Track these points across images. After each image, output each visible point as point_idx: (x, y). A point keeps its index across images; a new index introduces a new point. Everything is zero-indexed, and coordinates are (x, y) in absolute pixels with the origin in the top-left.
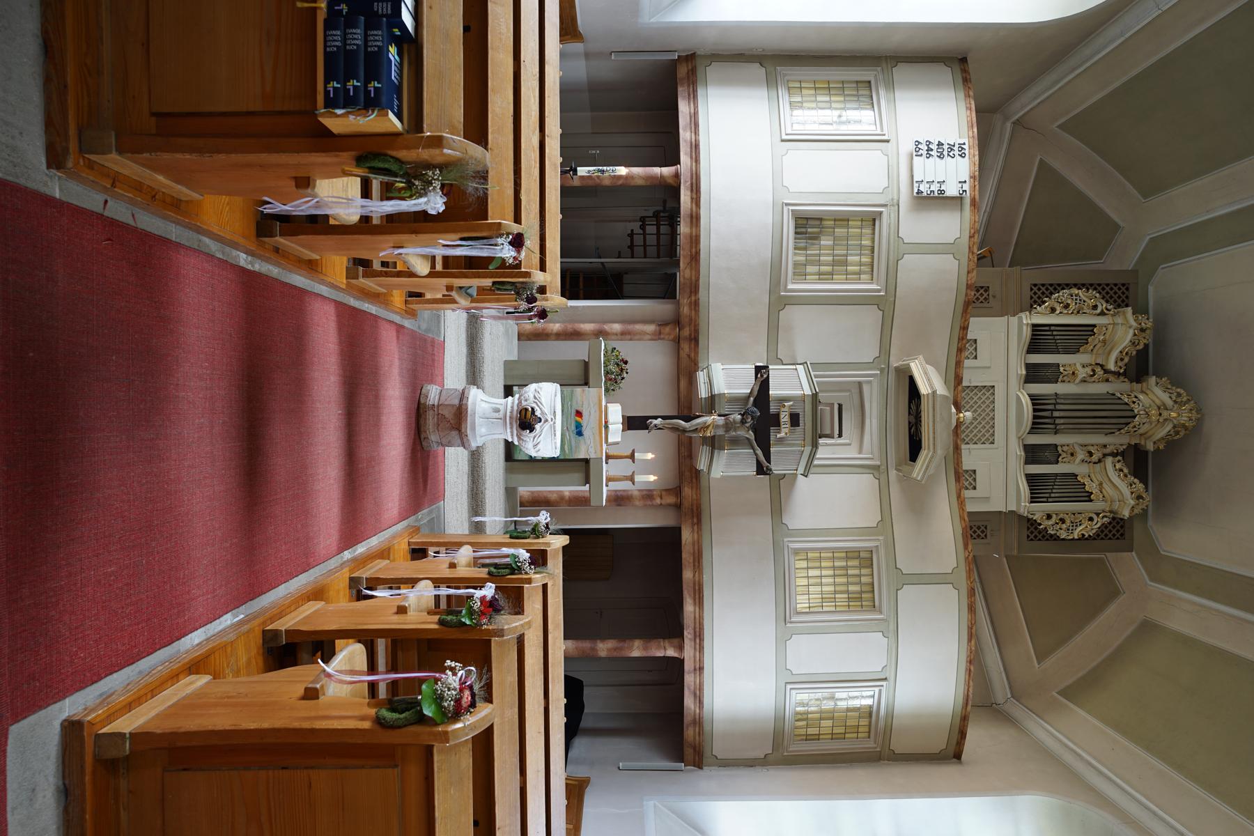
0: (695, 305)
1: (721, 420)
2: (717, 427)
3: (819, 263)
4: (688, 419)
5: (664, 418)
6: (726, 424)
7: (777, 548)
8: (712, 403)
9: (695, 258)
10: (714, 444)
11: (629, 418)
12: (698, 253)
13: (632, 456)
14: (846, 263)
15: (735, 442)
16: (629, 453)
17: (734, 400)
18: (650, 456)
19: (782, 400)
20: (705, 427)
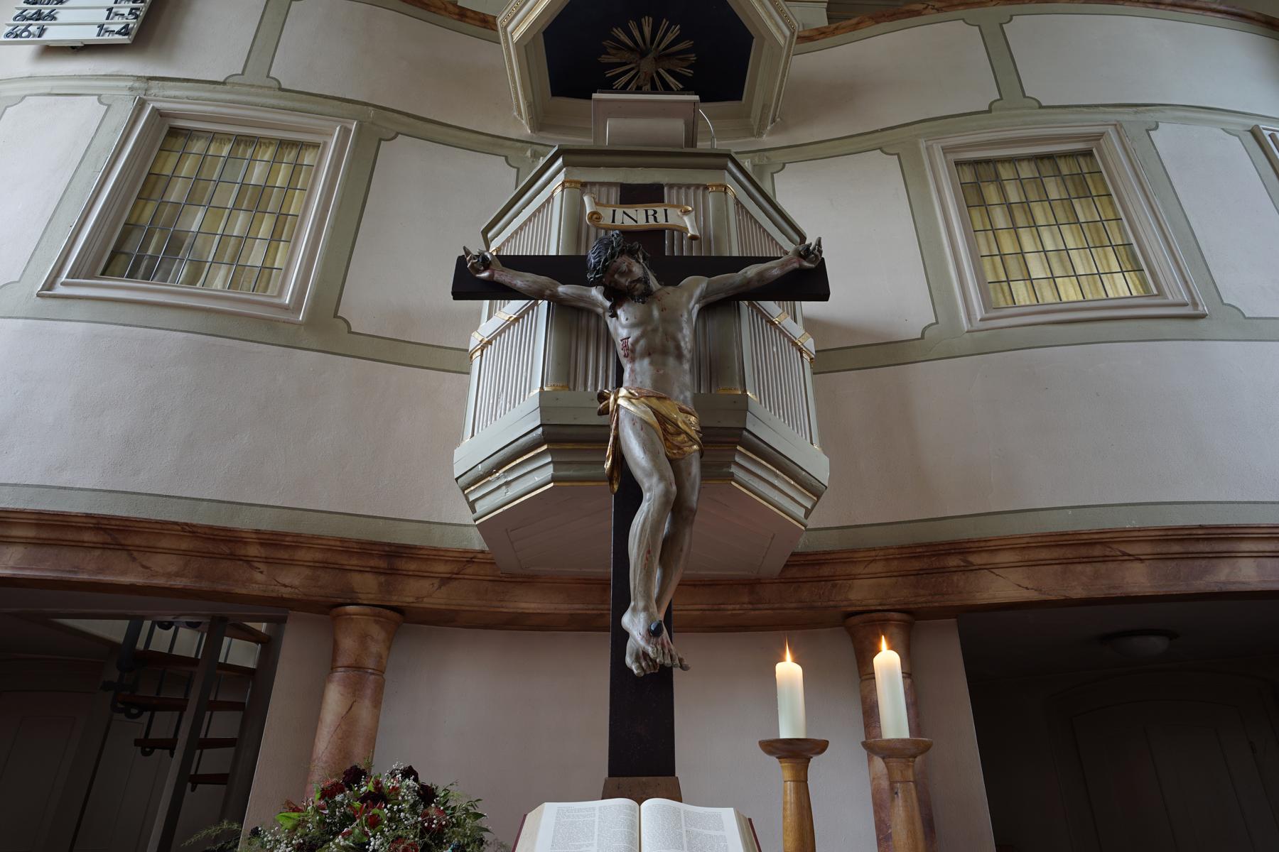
0: (278, 545)
1: (638, 372)
2: (659, 392)
3: (244, 240)
4: (629, 495)
5: (622, 603)
6: (649, 352)
7: (983, 345)
8: (570, 436)
9: (113, 533)
10: (725, 438)
11: (613, 772)
12: (99, 524)
13: (798, 753)
14: (262, 191)
15: (716, 368)
16: (779, 773)
17: (565, 368)
18: (789, 670)
19: (576, 225)
20: (662, 430)
